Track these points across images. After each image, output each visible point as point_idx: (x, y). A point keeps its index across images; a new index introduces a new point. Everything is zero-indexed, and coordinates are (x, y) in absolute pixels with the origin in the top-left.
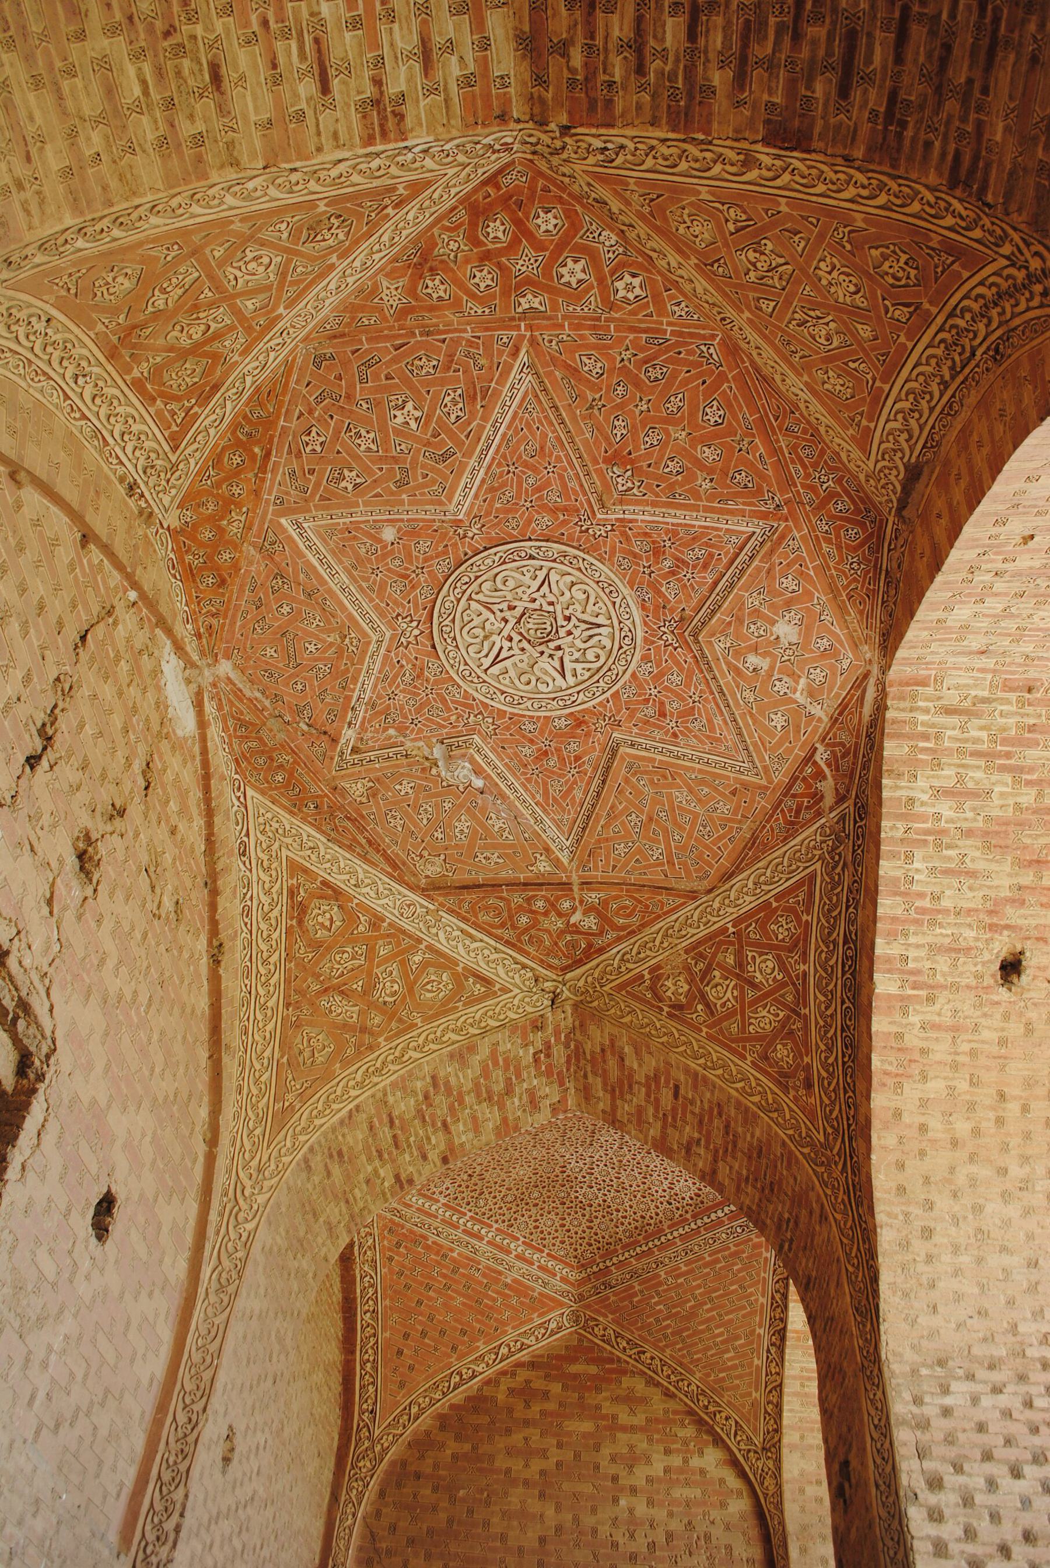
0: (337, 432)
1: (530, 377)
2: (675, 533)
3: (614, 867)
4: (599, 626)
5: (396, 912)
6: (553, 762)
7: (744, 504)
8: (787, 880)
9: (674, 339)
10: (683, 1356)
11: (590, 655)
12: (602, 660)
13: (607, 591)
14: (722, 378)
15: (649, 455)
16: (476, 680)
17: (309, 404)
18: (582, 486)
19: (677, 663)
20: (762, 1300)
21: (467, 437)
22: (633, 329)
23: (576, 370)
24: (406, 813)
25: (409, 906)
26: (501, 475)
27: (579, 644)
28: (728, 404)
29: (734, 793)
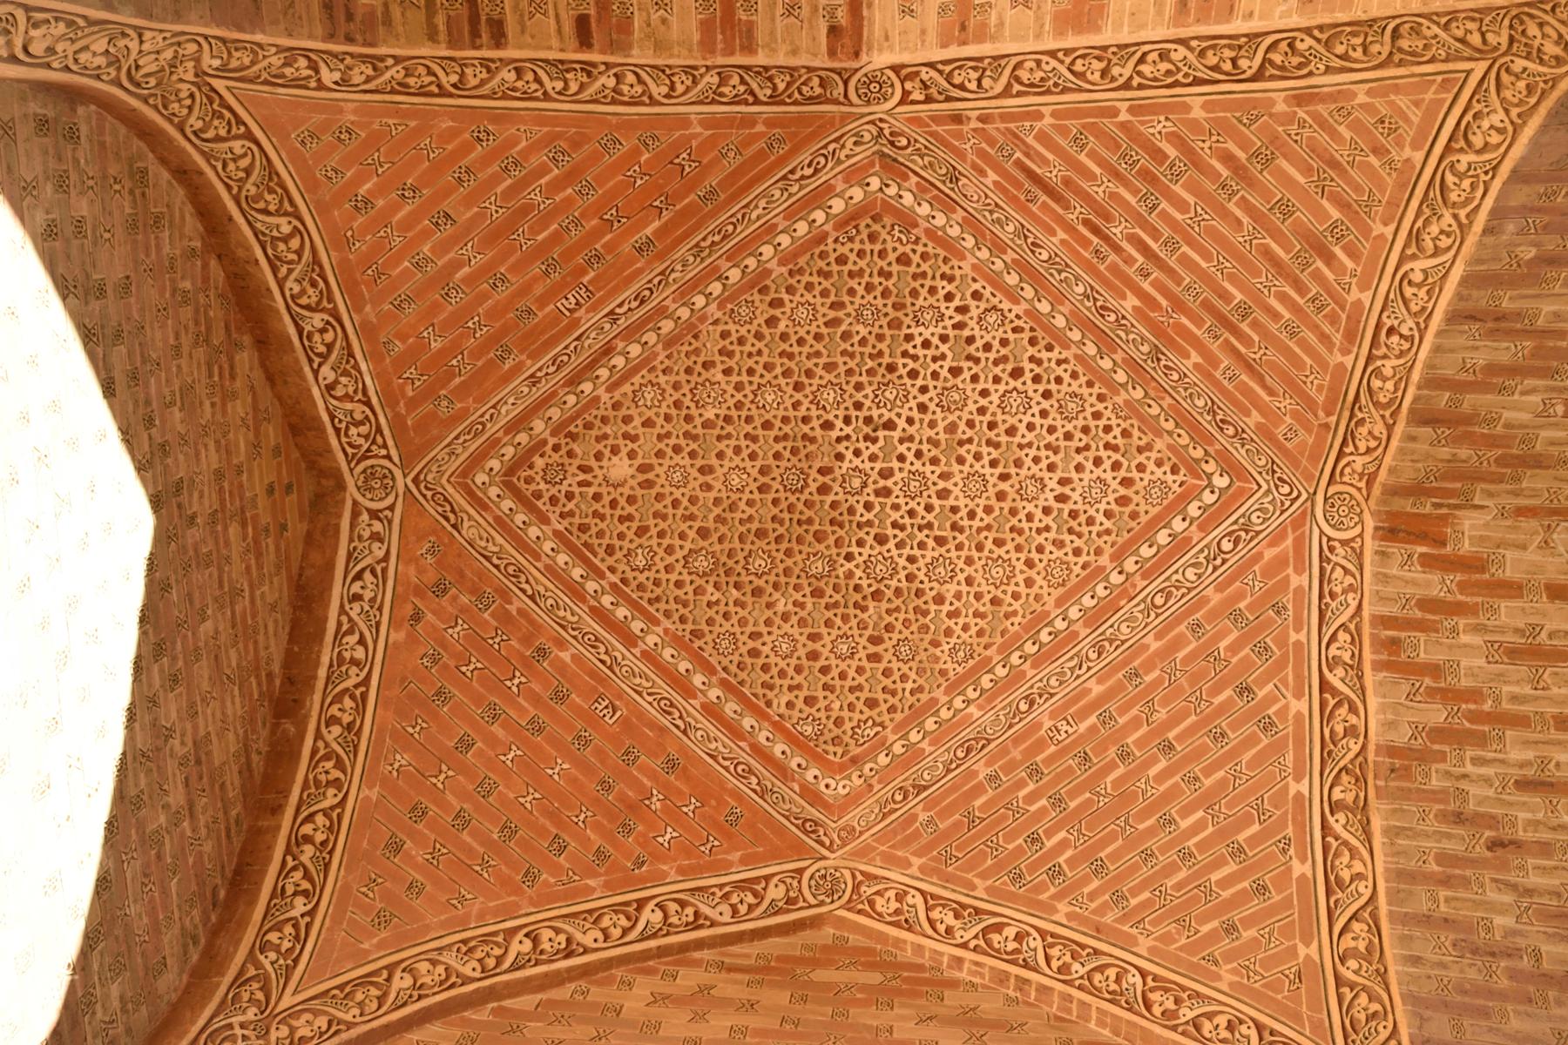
10: (1101, 911)
20: (1298, 706)
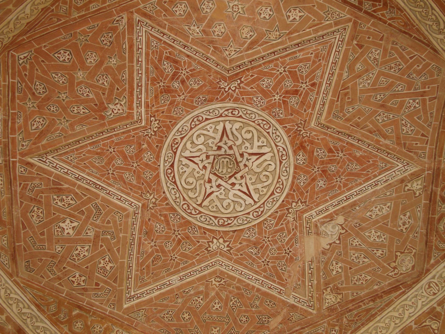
0: (74, 266)
1: (49, 157)
2: (154, 80)
3: (423, 135)
4: (224, 129)
5: (432, 297)
6: (332, 168)
7: (124, 38)
8: (433, 9)
9: (17, 78)
11: (249, 136)
13: (197, 123)
14: (39, 51)
15: (97, 94)
17: (55, 278)
18: (123, 133)
19: (254, 81)
21: (85, 196)
22: (13, 100)
23: (42, 132)
24: (357, 271)
25: (430, 287)
26: (115, 178)
27: (238, 143)
28: (56, 48)
29: (361, 46)
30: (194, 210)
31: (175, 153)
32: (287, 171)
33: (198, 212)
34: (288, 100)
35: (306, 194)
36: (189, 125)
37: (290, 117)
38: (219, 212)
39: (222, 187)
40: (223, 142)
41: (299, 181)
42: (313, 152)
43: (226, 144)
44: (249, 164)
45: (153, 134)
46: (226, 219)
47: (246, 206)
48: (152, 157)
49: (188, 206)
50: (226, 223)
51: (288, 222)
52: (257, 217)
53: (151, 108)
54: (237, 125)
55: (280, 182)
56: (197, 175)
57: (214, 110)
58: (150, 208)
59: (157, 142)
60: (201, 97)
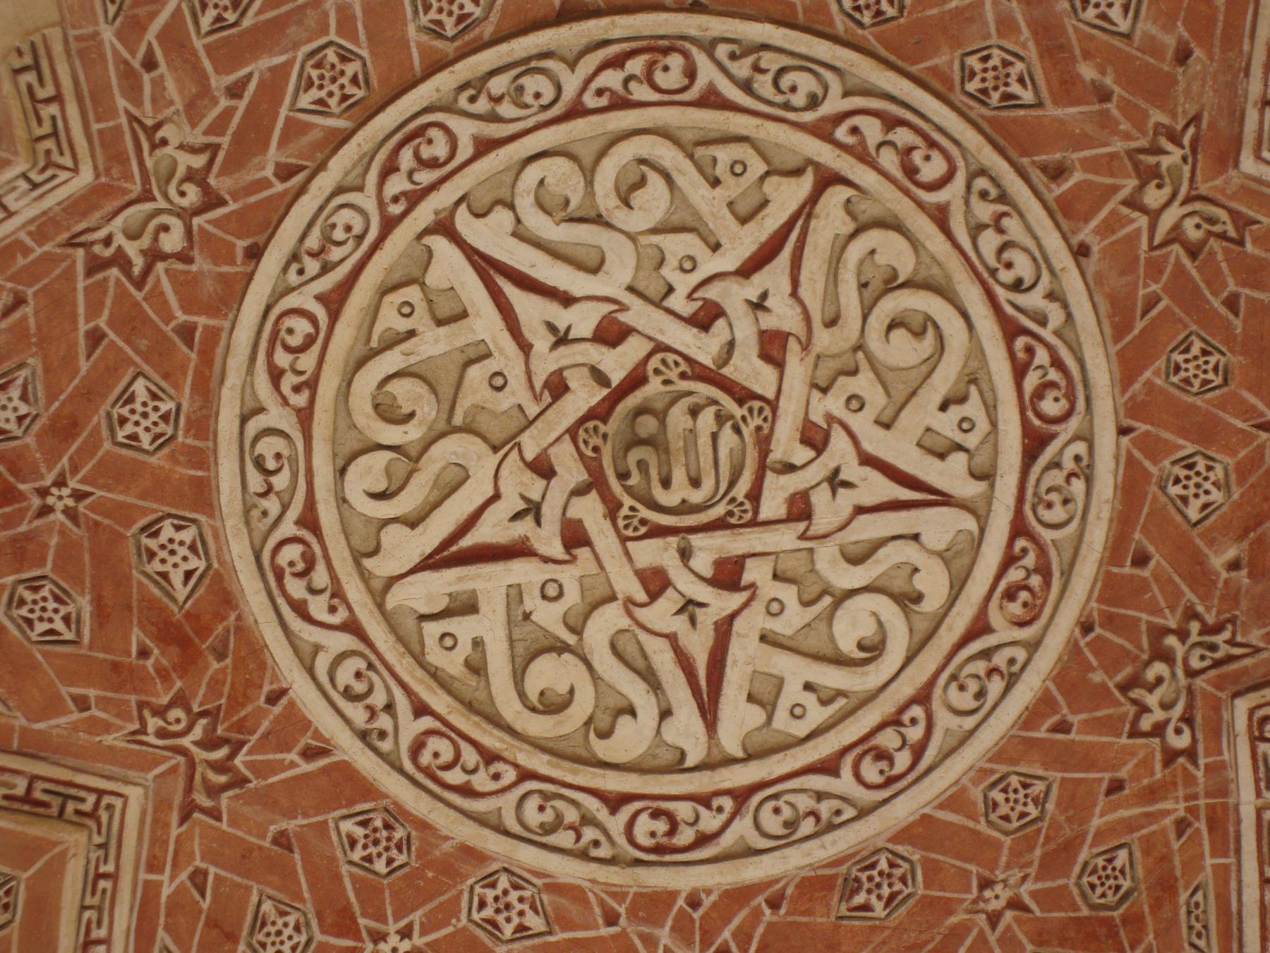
4: (709, 712)
11: (549, 674)
12: (538, 726)
13: (888, 739)
16: (397, 184)
30: (872, 143)
31: (1019, 528)
32: (259, 463)
33: (841, 133)
34: (319, 937)
35: (102, 322)
36: (944, 720)
37: (291, 825)
38: (688, 136)
39: (687, 309)
40: (707, 619)
41: (165, 407)
42: (101, 613)
43: (689, 607)
44: (519, 484)
45: (1171, 641)
46: (641, 92)
47: (504, 193)
48: (1175, 490)
49: (911, 172)
50: (636, 66)
51: (193, 112)
52: (420, 132)
53: (1192, 811)
54: (631, 739)
55: (297, 389)
56: (863, 383)
57: (788, 837)
58: (1175, 139)
59: (1144, 586)
60: (878, 906)
